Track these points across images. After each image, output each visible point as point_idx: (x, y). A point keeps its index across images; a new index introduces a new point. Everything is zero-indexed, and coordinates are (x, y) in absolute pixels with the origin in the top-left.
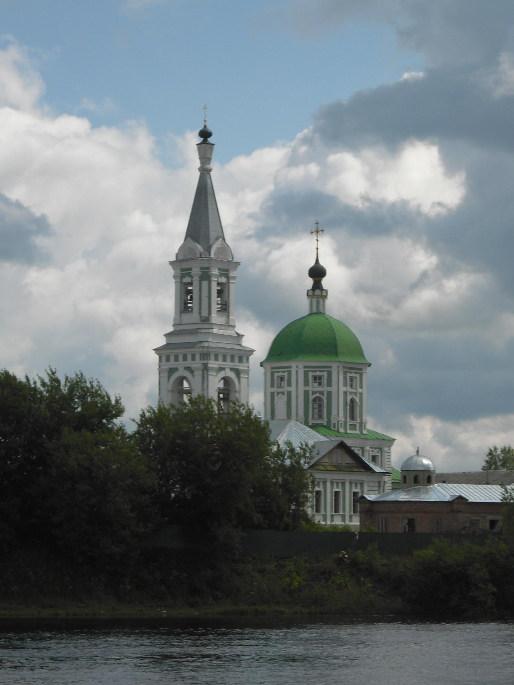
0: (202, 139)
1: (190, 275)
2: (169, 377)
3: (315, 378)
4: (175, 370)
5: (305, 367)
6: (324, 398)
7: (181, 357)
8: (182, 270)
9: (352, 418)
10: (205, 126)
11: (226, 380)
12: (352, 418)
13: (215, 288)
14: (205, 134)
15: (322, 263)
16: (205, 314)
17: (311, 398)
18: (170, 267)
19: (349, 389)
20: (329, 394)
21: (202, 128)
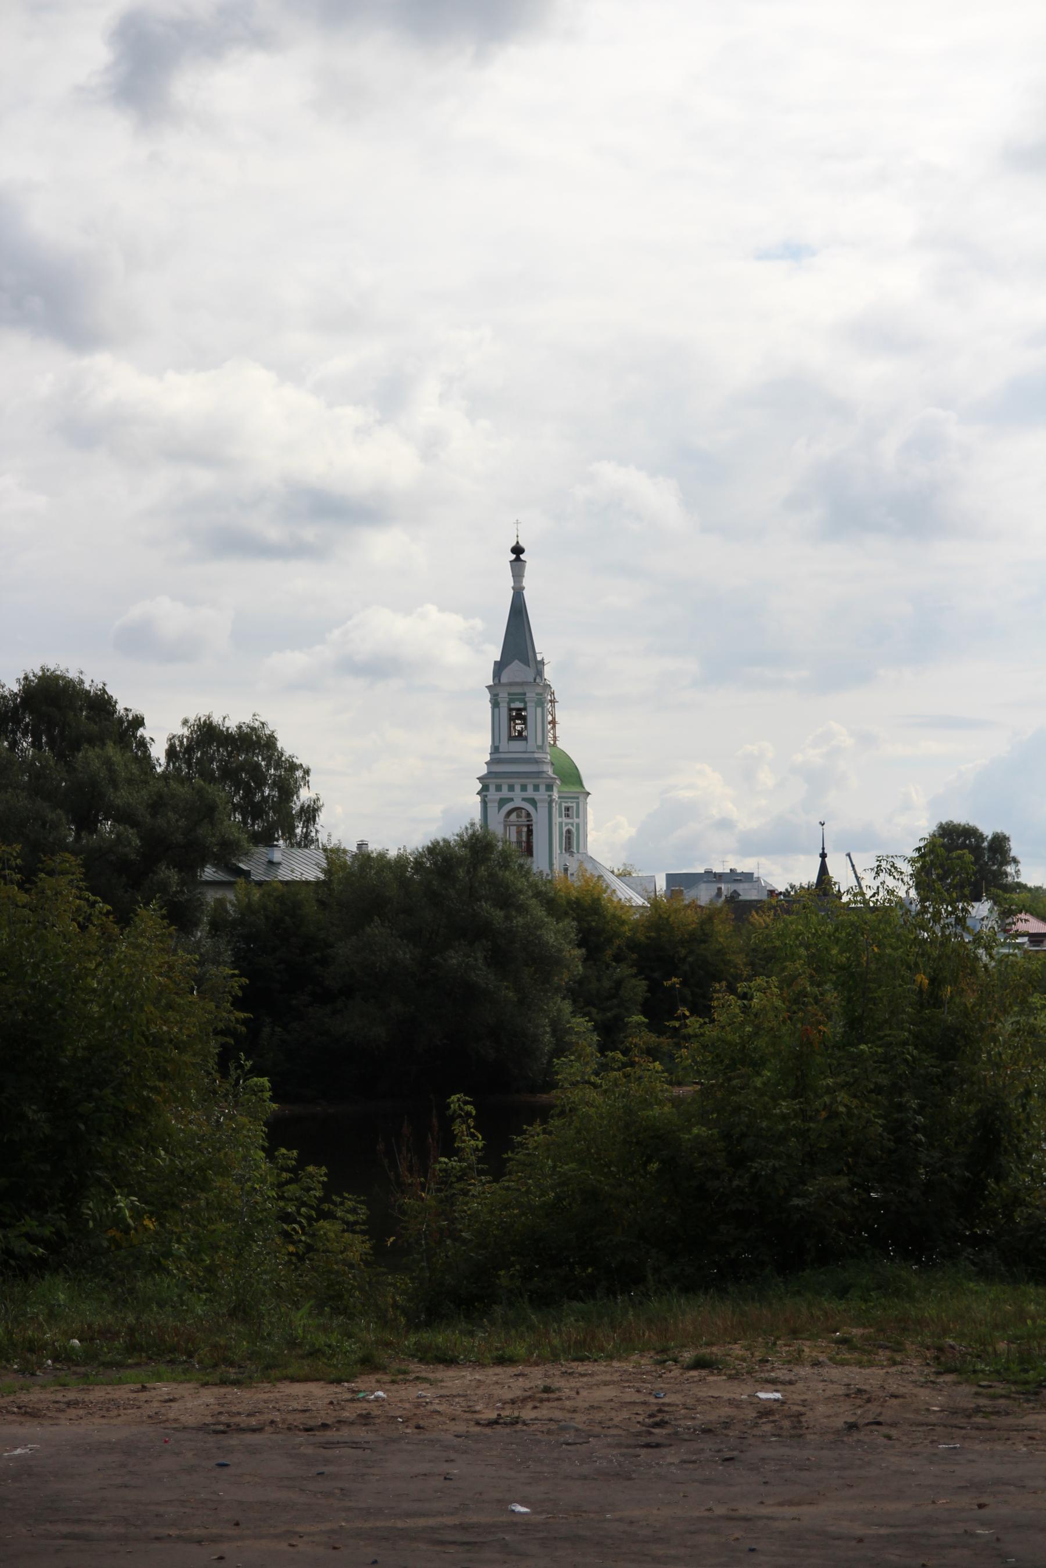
0: (514, 556)
2: (499, 809)
6: (574, 830)
7: (518, 788)
8: (509, 694)
14: (518, 550)
16: (539, 743)
17: (565, 829)
18: (487, 690)
20: (578, 825)
21: (514, 544)
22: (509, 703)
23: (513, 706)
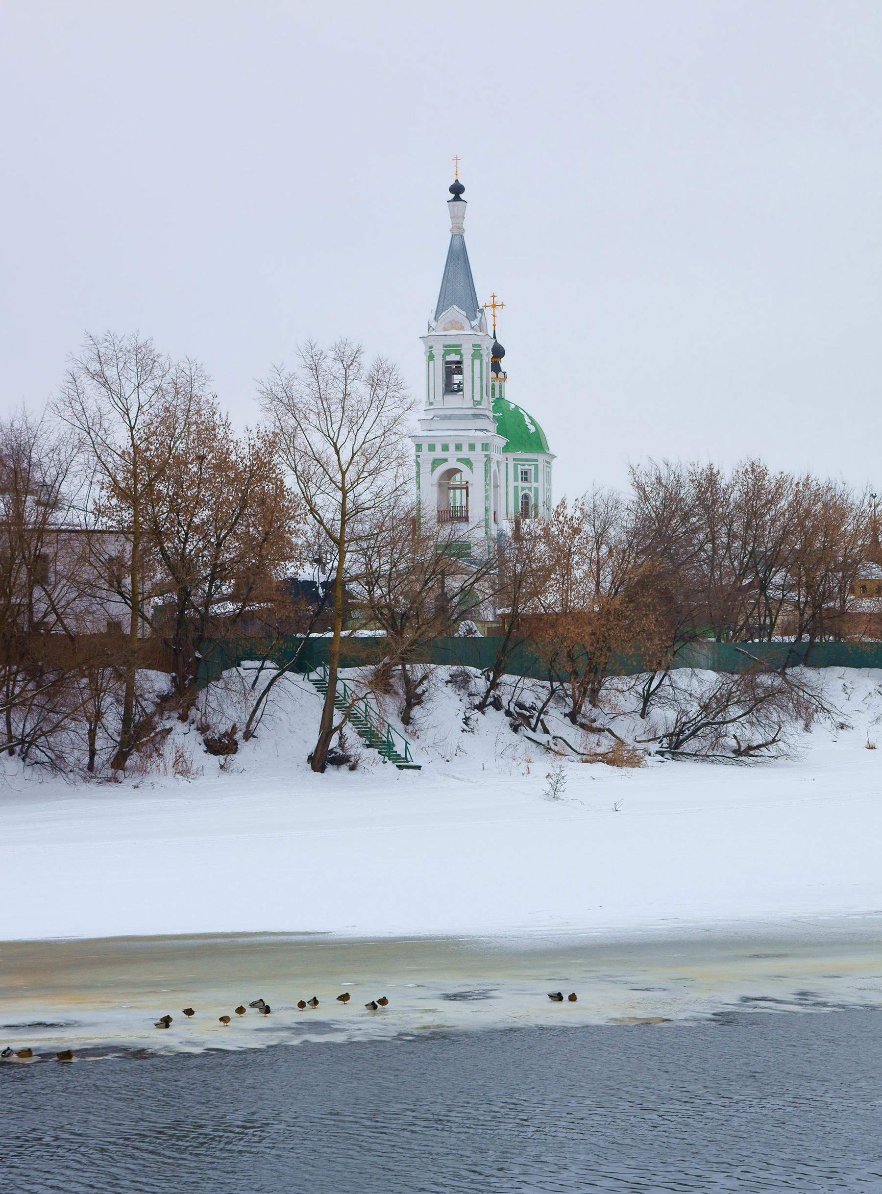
1: (458, 352)
2: (433, 470)
5: (514, 460)
6: (532, 495)
10: (457, 181)
14: (457, 190)
17: (520, 495)
20: (536, 489)
21: (453, 182)
22: (444, 356)
23: (449, 358)
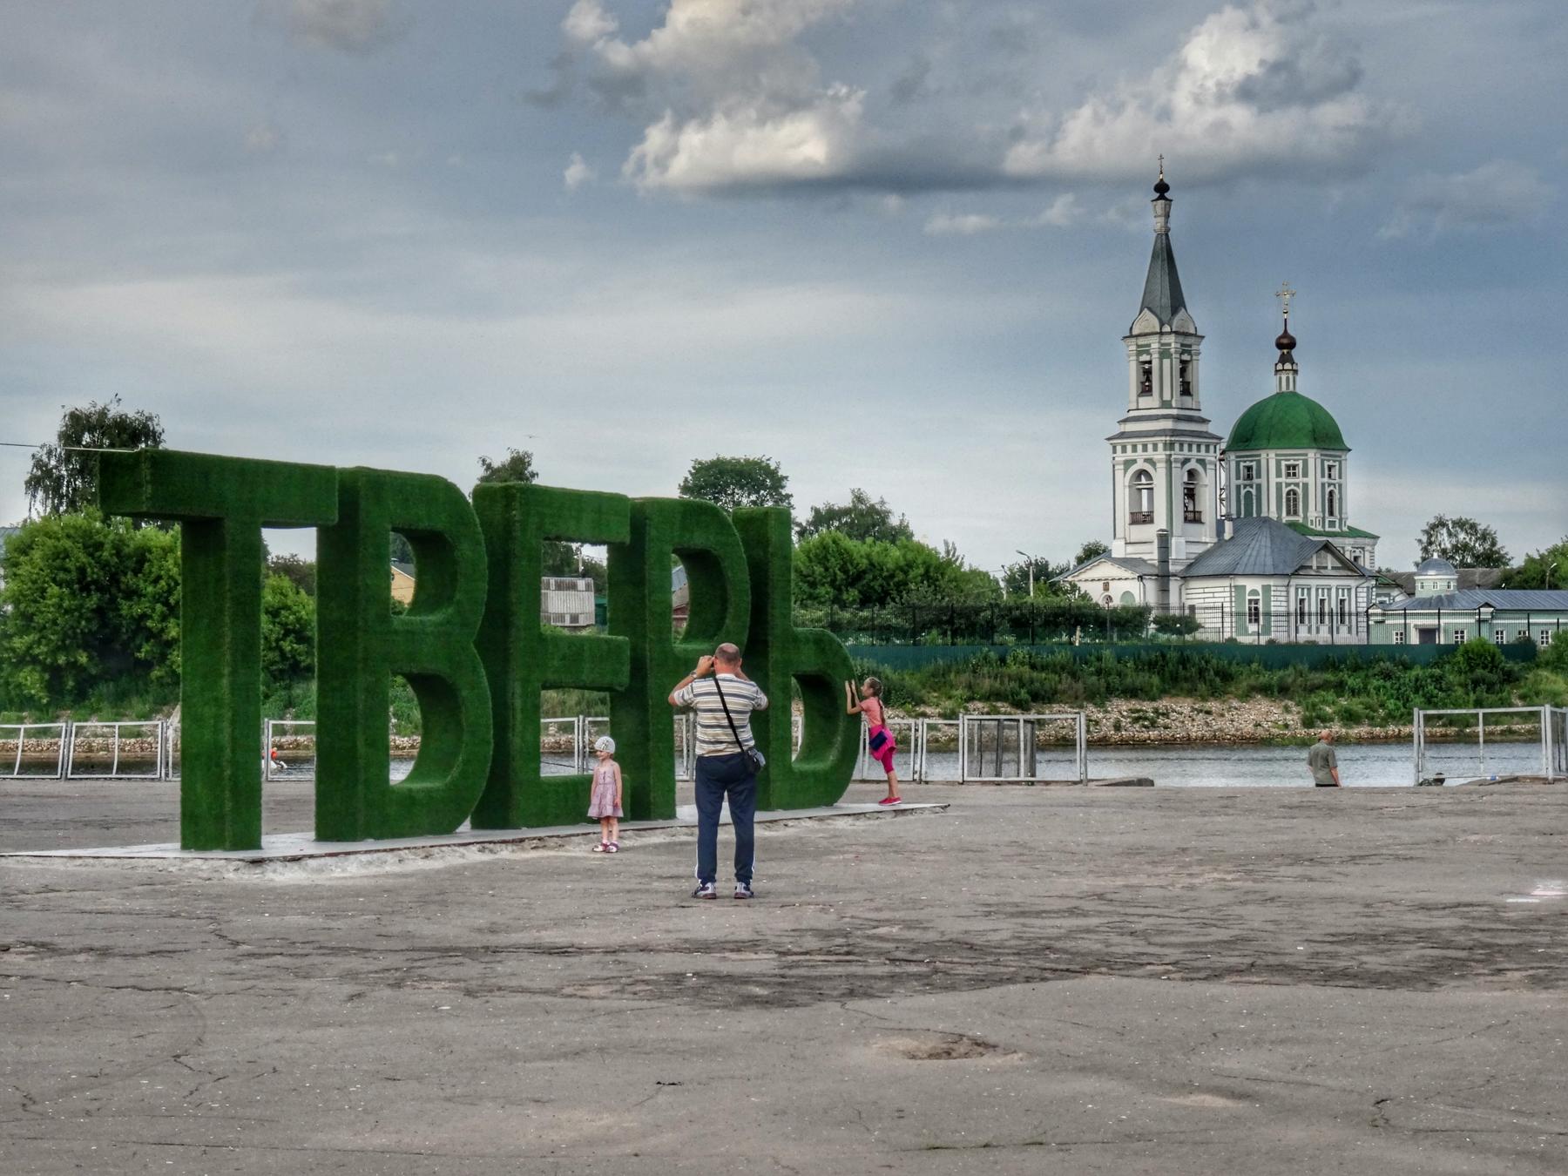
1: (1148, 352)
2: (1125, 471)
3: (1288, 467)
4: (1134, 461)
6: (1300, 491)
7: (1140, 447)
9: (1331, 513)
11: (1192, 474)
12: (1331, 513)
13: (1177, 366)
15: (1291, 332)
16: (1167, 397)
17: (1285, 491)
19: (1326, 479)
20: (1306, 486)
